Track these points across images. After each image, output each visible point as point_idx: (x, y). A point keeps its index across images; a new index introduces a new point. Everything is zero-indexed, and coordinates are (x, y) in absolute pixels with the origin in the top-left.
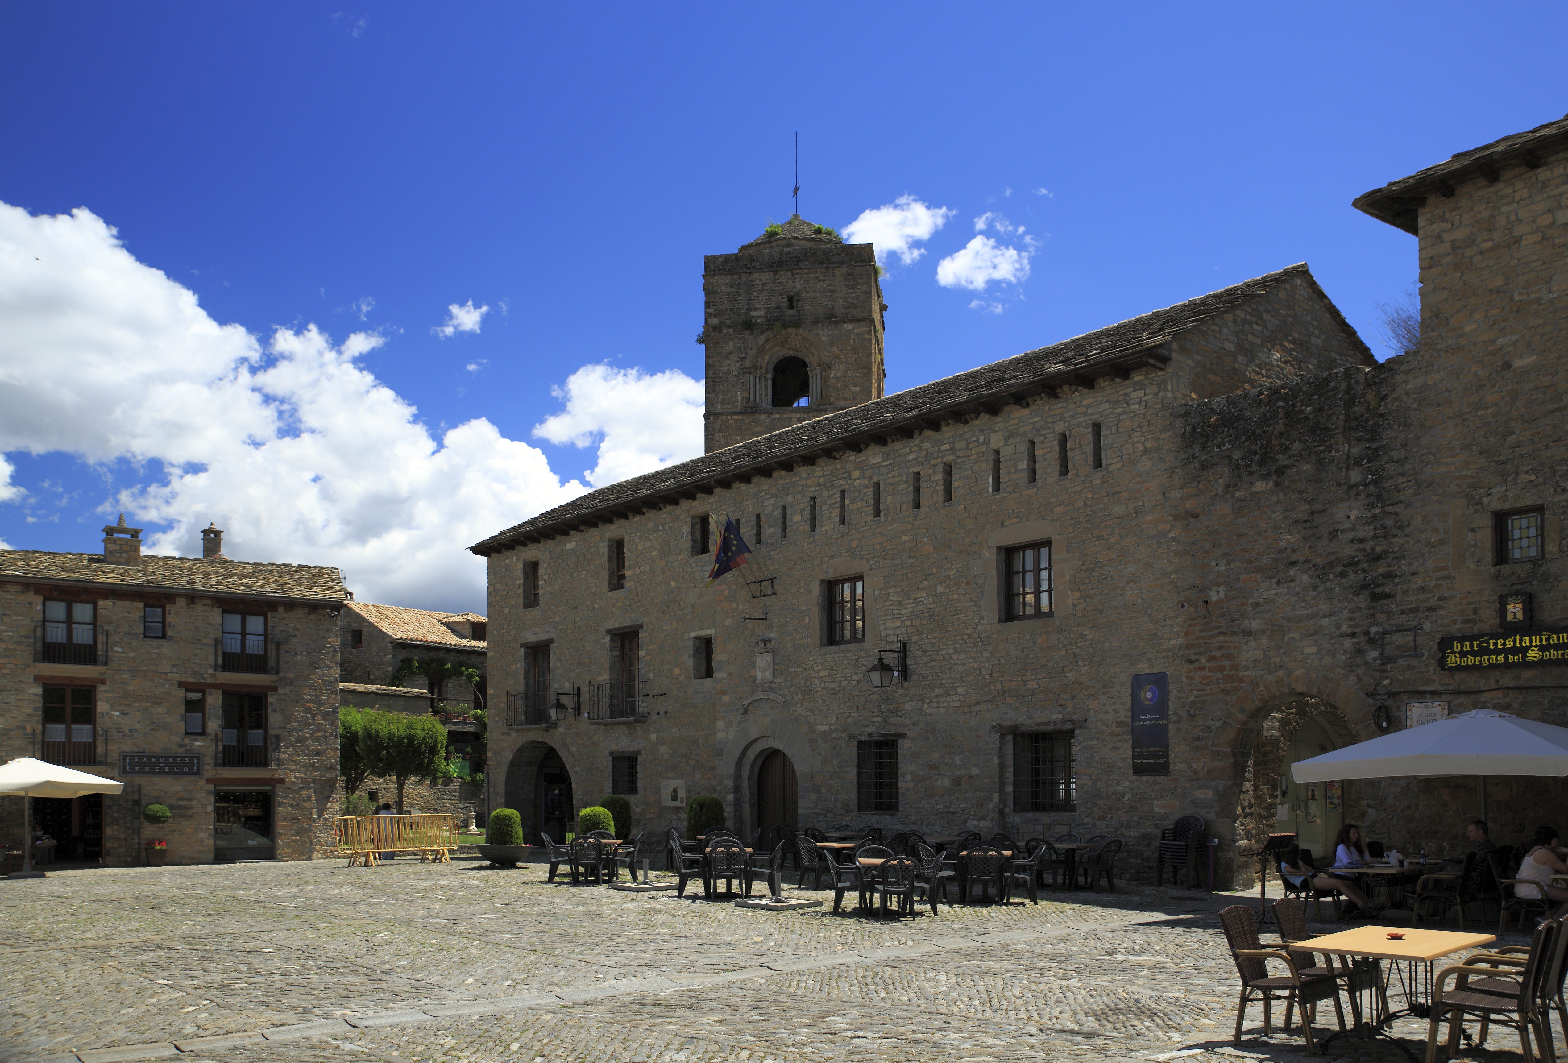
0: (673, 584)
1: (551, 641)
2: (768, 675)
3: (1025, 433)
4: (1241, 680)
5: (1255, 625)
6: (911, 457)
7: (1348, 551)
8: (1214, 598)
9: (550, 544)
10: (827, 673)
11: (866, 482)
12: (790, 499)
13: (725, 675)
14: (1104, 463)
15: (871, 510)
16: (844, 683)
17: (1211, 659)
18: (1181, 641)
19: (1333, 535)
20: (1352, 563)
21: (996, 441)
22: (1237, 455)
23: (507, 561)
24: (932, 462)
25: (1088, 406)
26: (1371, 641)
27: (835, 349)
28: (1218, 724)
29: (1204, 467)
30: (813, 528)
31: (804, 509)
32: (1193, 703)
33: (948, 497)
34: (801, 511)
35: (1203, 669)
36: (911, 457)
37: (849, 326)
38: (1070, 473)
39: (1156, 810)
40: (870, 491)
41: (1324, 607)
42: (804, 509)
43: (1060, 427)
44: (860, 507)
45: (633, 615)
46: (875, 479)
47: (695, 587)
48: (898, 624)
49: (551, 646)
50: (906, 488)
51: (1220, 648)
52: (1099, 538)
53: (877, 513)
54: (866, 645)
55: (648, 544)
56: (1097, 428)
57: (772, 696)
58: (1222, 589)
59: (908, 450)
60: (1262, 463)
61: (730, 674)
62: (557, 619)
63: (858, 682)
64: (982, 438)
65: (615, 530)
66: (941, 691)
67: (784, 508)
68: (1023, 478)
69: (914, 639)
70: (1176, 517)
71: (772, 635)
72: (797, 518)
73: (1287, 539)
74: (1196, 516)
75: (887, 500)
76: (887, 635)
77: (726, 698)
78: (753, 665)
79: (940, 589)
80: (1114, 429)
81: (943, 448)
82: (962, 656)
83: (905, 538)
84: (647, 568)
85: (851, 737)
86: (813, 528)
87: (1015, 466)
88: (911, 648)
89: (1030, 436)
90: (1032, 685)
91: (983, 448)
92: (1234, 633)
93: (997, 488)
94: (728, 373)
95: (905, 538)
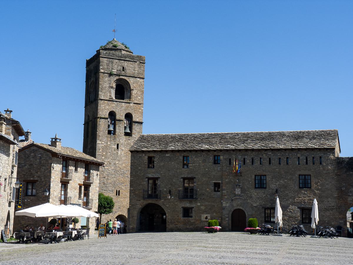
0: (207, 169)
1: (159, 178)
2: (239, 193)
3: (305, 155)
4: (348, 203)
6: (279, 154)
8: (343, 189)
10: (256, 194)
11: (267, 157)
12: (246, 157)
13: (226, 192)
14: (322, 164)
15: (268, 163)
16: (261, 196)
17: (342, 199)
18: (337, 196)
21: (299, 155)
22: (347, 167)
23: (140, 155)
24: (284, 156)
25: (319, 153)
27: (134, 85)
28: (344, 210)
30: (253, 164)
31: (250, 160)
32: (339, 206)
33: (287, 164)
34: (249, 160)
35: (341, 200)
36: (279, 154)
38: (315, 164)
39: (333, 224)
40: (268, 159)
42: (250, 160)
43: (313, 156)
44: (266, 162)
45: (192, 175)
46: (269, 157)
47: (215, 171)
48: (275, 186)
49: (159, 179)
50: (277, 160)
51: (344, 197)
52: (321, 176)
53: (270, 163)
54: (267, 189)
55: (199, 159)
56: (321, 157)
57: (241, 197)
58: (344, 188)
59: (278, 153)
61: (227, 192)
62: (162, 172)
63: (265, 196)
64: (295, 154)
65: (185, 154)
66: (285, 200)
67: (244, 159)
68: (305, 163)
69: (279, 189)
70: (336, 175)
71: (240, 185)
72: (248, 161)
74: (340, 175)
75: (272, 161)
76: (272, 188)
78: (235, 190)
79: (286, 181)
80: (324, 158)
81: (286, 154)
82: (291, 194)
83: (277, 170)
84: (198, 165)
85: (263, 207)
86: (253, 164)
87: (303, 161)
88: (278, 191)
89: (307, 156)
91: (296, 156)
92: (346, 195)
93: (299, 164)
94: (105, 87)
95: (277, 170)
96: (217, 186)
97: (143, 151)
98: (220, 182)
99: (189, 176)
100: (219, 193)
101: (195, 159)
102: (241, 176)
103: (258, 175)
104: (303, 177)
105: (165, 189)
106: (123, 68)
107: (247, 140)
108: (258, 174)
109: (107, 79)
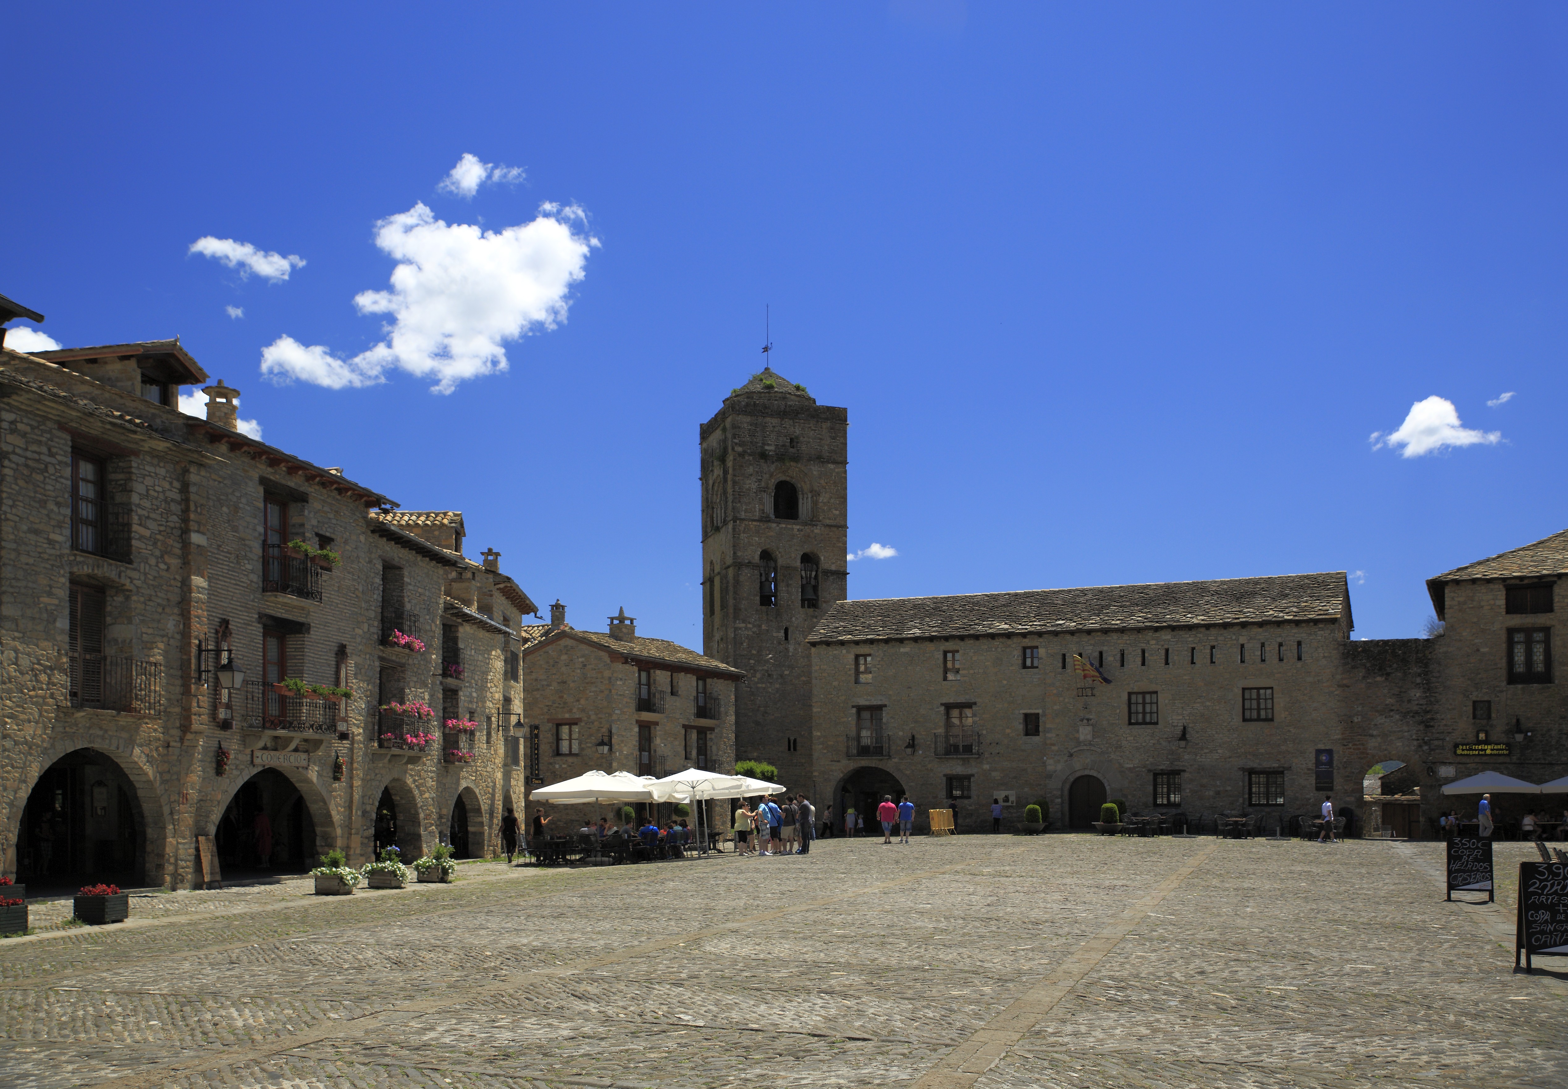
1: (885, 706)
2: (1089, 737)
5: (1375, 733)
7: (1415, 708)
9: (886, 647)
18: (1339, 736)
19: (1409, 701)
20: (1417, 713)
26: (1425, 743)
29: (1354, 667)
30: (1122, 665)
34: (1114, 656)
37: (831, 466)
41: (1405, 728)
44: (1155, 658)
53: (1167, 663)
54: (1159, 726)
60: (1380, 669)
72: (1111, 659)
73: (1389, 701)
77: (1054, 748)
78: (1078, 732)
79: (1208, 703)
84: (981, 671)
85: (1149, 771)
90: (1262, 751)
96: (1032, 725)
97: (842, 643)
98: (1040, 711)
99: (961, 699)
100: (1036, 739)
101: (975, 658)
102: (1093, 695)
103: (1137, 693)
104: (1254, 693)
105: (901, 733)
106: (792, 440)
107: (1107, 607)
108: (1136, 690)
109: (751, 470)
